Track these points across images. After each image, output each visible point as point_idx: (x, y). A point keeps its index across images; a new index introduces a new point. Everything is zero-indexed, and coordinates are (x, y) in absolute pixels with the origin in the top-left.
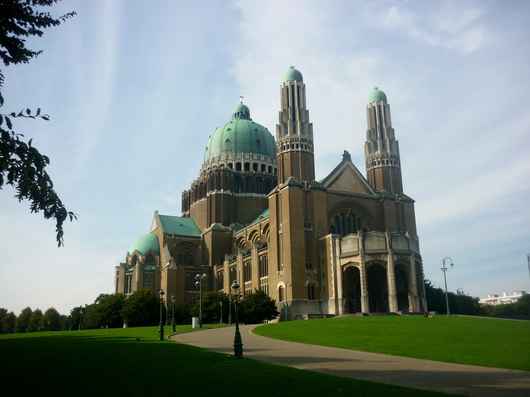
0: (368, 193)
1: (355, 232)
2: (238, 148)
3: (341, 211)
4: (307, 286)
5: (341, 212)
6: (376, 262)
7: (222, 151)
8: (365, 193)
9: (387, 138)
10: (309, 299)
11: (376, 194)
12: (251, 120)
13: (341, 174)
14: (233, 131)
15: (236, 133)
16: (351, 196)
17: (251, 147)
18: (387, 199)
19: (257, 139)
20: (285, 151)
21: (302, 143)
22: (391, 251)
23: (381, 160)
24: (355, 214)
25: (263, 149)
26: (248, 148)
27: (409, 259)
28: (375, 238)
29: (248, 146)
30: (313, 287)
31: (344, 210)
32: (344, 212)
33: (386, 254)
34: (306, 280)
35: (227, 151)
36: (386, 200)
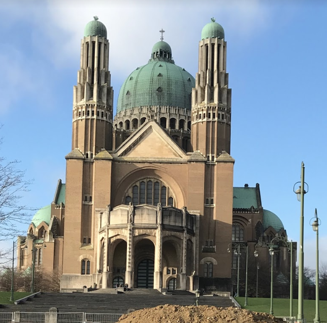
0: (176, 156)
1: (126, 203)
2: (136, 101)
3: (141, 179)
4: (80, 261)
5: (141, 181)
6: (118, 237)
7: (122, 106)
8: (173, 157)
9: (216, 86)
10: (82, 274)
11: (187, 156)
12: (173, 62)
13: (141, 137)
14: (134, 80)
15: (136, 82)
16: (151, 163)
17: (151, 98)
18: (193, 162)
19: (160, 86)
20: (80, 118)
21: (98, 110)
22: (131, 226)
23: (207, 112)
24: (158, 181)
25: (166, 99)
26: (148, 99)
27: (155, 233)
28: (119, 213)
29: (148, 96)
30: (89, 262)
31: (145, 178)
32: (145, 181)
33: (126, 228)
34: (79, 255)
35: (127, 105)
36: (192, 163)
